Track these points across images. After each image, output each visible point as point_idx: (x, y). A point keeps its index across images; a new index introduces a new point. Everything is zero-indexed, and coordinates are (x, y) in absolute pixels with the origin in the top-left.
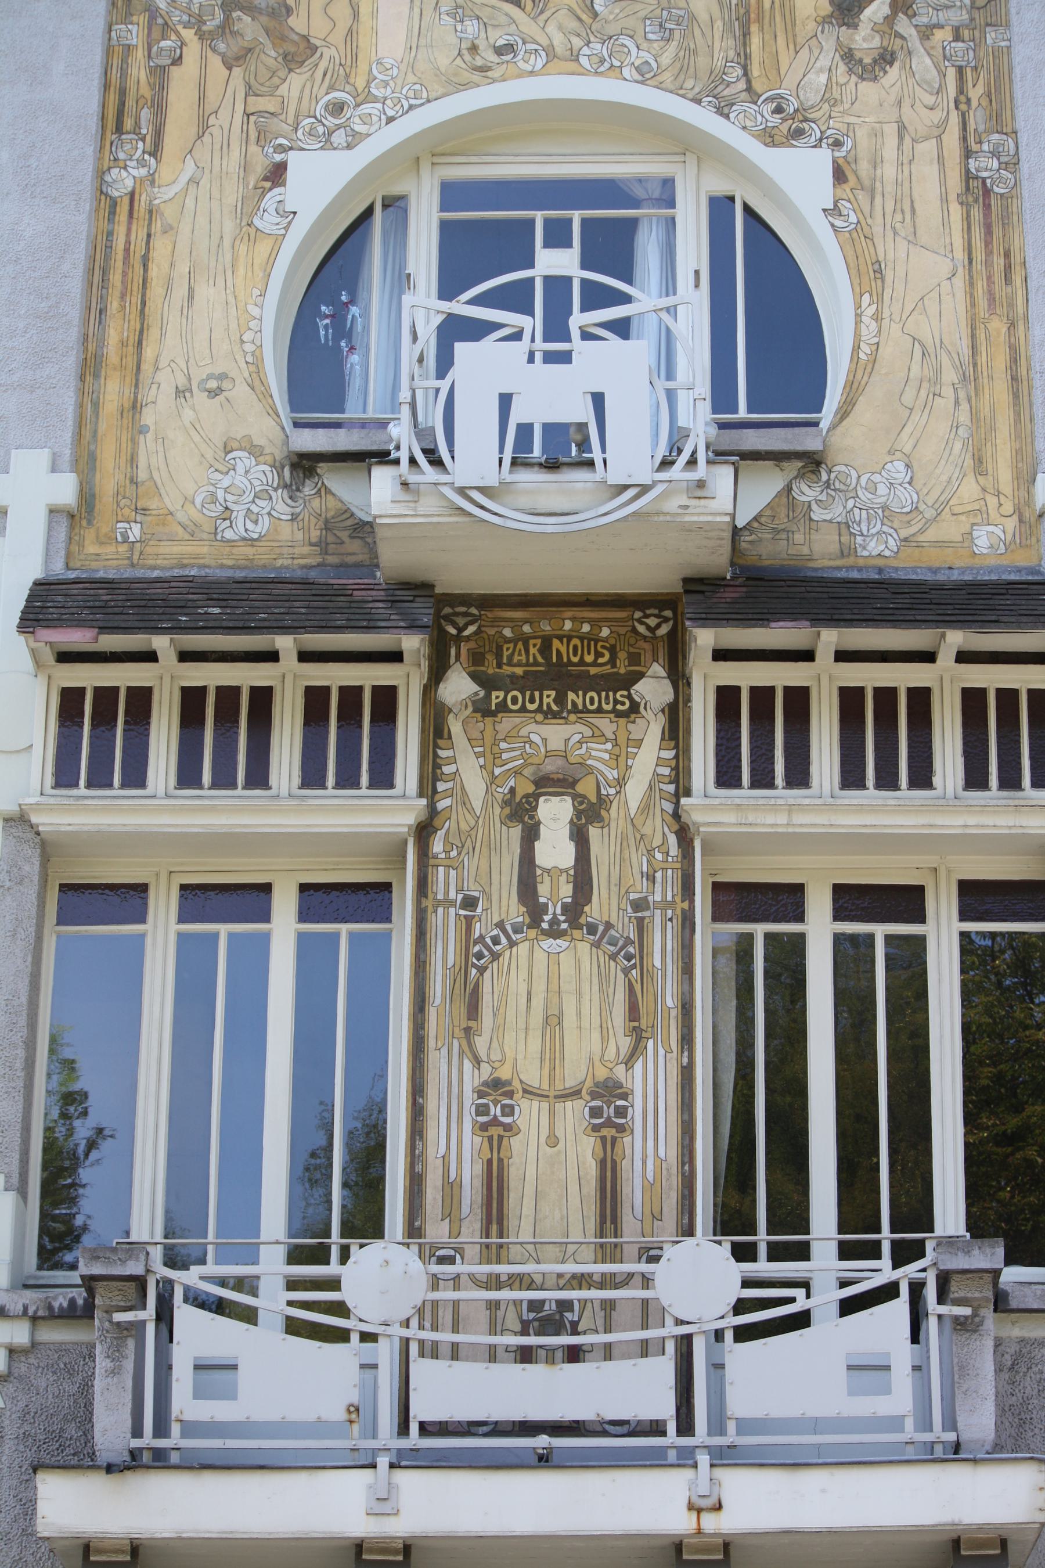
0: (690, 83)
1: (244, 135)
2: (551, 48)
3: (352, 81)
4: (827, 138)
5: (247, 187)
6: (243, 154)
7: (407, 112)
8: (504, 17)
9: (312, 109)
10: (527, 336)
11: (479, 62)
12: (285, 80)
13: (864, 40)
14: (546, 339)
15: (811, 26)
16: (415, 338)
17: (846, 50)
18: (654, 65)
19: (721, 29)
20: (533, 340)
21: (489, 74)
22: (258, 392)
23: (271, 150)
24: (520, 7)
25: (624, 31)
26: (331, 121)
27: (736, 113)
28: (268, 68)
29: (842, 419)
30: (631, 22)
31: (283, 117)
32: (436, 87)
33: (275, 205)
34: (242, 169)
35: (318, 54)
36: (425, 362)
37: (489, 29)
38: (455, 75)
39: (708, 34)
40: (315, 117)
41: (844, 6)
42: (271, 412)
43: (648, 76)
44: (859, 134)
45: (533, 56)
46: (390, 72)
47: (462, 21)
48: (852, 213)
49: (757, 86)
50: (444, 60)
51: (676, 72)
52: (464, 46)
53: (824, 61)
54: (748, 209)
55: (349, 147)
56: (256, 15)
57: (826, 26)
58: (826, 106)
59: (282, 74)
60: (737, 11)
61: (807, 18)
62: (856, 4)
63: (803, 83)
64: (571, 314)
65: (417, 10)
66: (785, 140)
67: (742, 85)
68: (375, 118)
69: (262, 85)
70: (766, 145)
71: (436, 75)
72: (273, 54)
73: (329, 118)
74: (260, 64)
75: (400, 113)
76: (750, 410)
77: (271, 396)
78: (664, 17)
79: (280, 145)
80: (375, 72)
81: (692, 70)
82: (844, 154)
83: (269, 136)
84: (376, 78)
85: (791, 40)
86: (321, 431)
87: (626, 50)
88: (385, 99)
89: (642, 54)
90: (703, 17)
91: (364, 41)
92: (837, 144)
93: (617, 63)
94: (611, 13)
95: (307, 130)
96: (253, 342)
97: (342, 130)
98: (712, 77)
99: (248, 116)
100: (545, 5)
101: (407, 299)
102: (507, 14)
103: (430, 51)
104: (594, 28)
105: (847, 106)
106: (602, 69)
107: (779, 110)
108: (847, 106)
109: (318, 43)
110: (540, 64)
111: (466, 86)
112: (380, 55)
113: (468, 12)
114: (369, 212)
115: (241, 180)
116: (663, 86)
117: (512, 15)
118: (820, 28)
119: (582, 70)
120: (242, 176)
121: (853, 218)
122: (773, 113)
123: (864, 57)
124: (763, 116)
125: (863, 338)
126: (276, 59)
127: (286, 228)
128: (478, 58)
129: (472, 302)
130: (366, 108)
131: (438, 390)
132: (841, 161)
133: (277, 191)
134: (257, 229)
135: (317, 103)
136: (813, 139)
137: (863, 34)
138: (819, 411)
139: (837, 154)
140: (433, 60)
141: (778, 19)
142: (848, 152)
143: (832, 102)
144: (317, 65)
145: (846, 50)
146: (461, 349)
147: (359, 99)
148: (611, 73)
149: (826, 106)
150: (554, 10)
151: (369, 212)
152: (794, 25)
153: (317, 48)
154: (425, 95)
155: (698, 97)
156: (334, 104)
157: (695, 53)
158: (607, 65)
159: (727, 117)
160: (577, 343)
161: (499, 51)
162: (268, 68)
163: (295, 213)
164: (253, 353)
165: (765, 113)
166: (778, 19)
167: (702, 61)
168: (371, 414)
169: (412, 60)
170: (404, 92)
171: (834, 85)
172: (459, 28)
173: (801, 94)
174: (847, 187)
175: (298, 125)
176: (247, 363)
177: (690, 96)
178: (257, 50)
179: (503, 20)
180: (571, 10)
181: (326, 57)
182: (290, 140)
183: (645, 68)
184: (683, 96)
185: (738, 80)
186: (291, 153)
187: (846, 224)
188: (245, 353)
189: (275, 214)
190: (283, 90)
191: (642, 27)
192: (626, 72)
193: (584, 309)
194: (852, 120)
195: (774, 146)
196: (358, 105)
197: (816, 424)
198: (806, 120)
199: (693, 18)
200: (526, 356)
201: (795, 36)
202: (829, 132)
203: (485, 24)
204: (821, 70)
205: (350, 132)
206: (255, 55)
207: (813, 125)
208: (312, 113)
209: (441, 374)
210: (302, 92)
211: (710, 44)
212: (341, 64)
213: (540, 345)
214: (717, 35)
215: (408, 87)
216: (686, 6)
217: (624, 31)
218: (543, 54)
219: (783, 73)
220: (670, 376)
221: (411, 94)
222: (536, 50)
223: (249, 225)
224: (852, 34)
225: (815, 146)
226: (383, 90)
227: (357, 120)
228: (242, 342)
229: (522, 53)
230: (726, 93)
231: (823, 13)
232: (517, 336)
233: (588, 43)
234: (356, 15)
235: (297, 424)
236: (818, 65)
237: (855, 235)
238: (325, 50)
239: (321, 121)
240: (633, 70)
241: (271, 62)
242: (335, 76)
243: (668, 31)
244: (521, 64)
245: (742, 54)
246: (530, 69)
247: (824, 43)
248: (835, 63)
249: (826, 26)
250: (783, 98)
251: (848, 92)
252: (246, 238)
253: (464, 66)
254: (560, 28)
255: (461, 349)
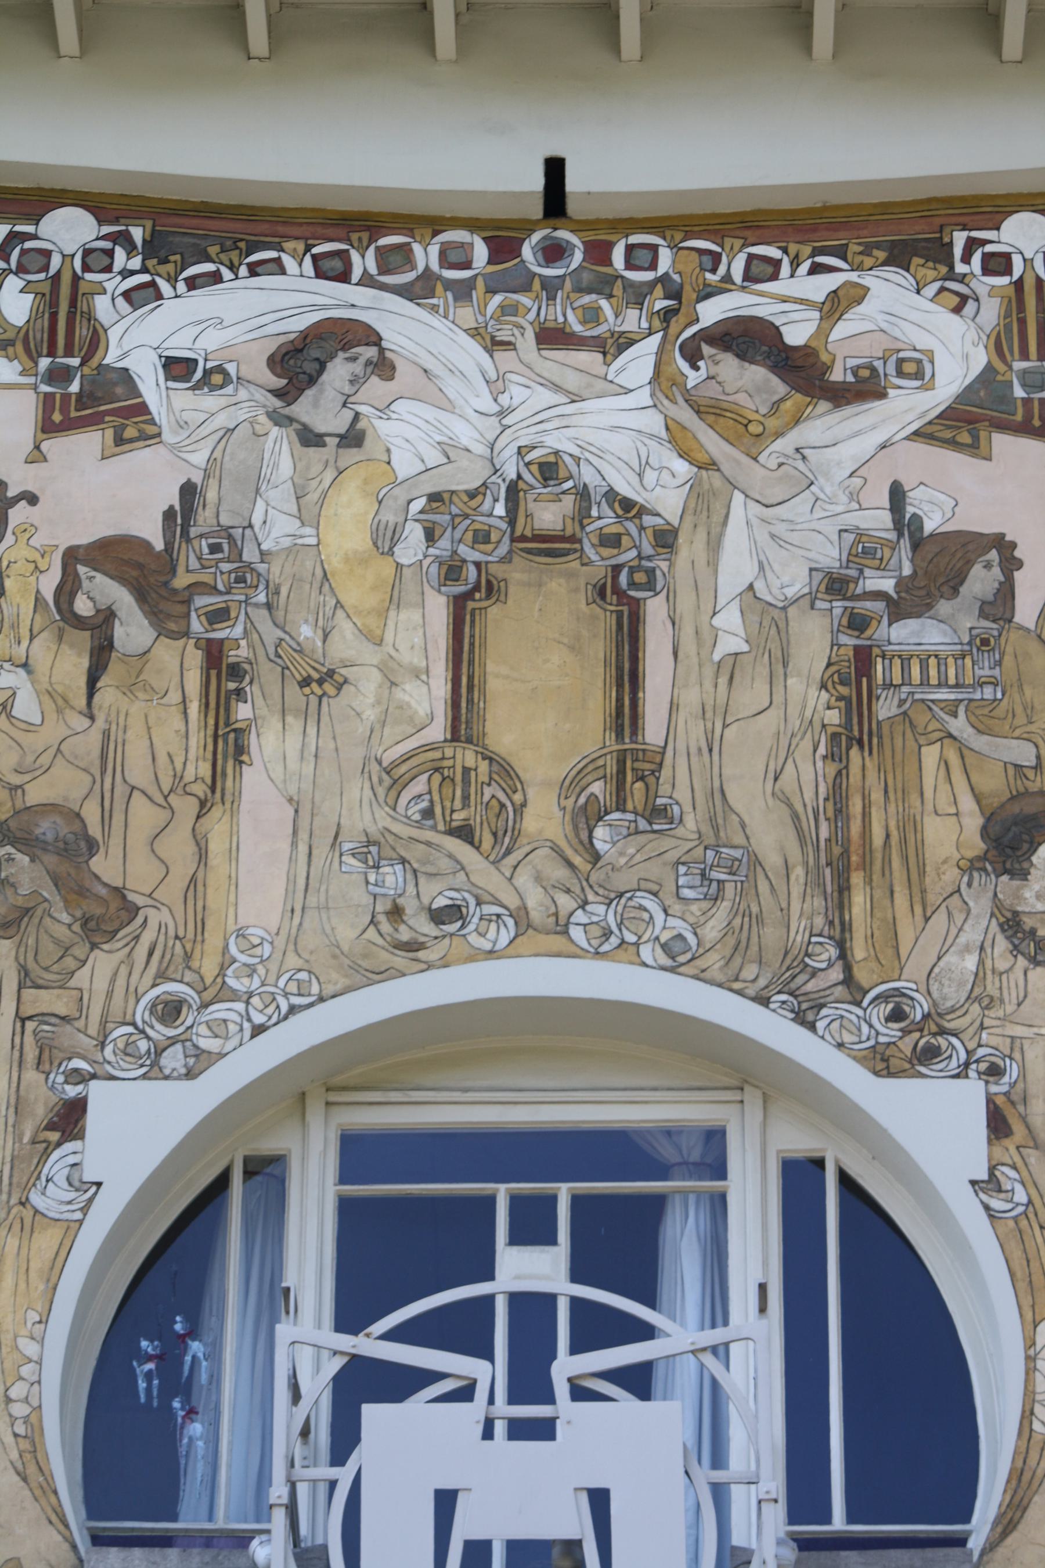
0: (750, 971)
1: (16, 1054)
2: (522, 913)
3: (195, 964)
4: (977, 1061)
5: (21, 1140)
6: (14, 1085)
7: (286, 1018)
8: (447, 860)
9: (129, 1012)
10: (481, 1393)
11: (405, 935)
12: (84, 962)
13: (1038, 897)
14: (514, 1399)
15: (951, 874)
16: (296, 1396)
17: (1009, 915)
18: (692, 940)
19: (802, 880)
20: (491, 1401)
21: (421, 954)
22: (34, 1485)
23: (61, 1079)
24: (472, 843)
25: (644, 885)
26: (160, 1032)
27: (827, 1021)
28: (57, 942)
29: (1005, 1534)
30: (654, 870)
31: (80, 1024)
32: (334, 976)
33: (66, 1171)
34: (12, 1110)
35: (139, 920)
36: (312, 1436)
37: (422, 880)
38: (365, 956)
39: (781, 888)
40: (134, 1024)
41: (1006, 840)
42: (54, 1518)
43: (682, 959)
44: (1029, 1055)
45: (493, 926)
46: (258, 951)
47: (377, 867)
48: (1018, 1187)
49: (861, 975)
50: (346, 932)
51: (728, 953)
52: (379, 908)
53: (972, 934)
54: (846, 1181)
55: (190, 1074)
56: (39, 852)
57: (976, 874)
58: (976, 1009)
59: (80, 951)
60: (829, 850)
61: (945, 862)
62: (1025, 837)
63: (936, 970)
64: (554, 1357)
65: (303, 848)
66: (907, 1066)
67: (836, 974)
68: (233, 1028)
69: (46, 969)
70: (877, 1073)
71: (334, 957)
72: (65, 918)
73: (158, 1026)
74: (44, 937)
75: (274, 1019)
76: (851, 1519)
77: (55, 1492)
78: (709, 862)
79: (76, 1070)
80: (233, 950)
81: (754, 948)
82: (1005, 1088)
83: (58, 1055)
84: (234, 961)
85: (917, 899)
86: (137, 1552)
87: (646, 916)
88: (251, 995)
89: (672, 922)
90: (772, 859)
91: (214, 899)
92: (994, 1072)
93: (631, 938)
94: (622, 854)
95: (121, 1044)
96: (26, 1400)
97: (179, 1047)
98: (788, 962)
99: (23, 1021)
100: (514, 840)
101: (284, 1331)
102: (451, 856)
103: (324, 916)
104: (593, 878)
105: (1010, 1008)
106: (606, 947)
107: (897, 1015)
108: (1010, 1008)
109: (140, 901)
110: (504, 939)
111: (383, 974)
112: (242, 922)
113: (387, 852)
114: (222, 1182)
115: (10, 1129)
116: (706, 975)
117: (460, 857)
118: (966, 879)
119: (574, 949)
120: (11, 1121)
121: (1021, 1196)
122: (889, 1019)
123: (1038, 925)
124: (871, 1026)
125: (1038, 1397)
126: (69, 926)
127: (85, 1210)
128: (402, 928)
129: (389, 1336)
130: (219, 1011)
131: (333, 1484)
132: (1000, 1101)
133: (69, 1147)
134: (36, 1211)
135: (138, 1001)
136: (954, 1063)
137: (1037, 887)
138: (967, 1519)
139: (994, 1089)
140: (328, 931)
141: (896, 863)
142: (1013, 1085)
143: (986, 1001)
144: (137, 938)
145: (1009, 915)
146: (372, 1414)
147: (208, 996)
148: (620, 951)
149: (976, 1009)
150: (528, 849)
151: (222, 1182)
152: (922, 873)
153: (138, 909)
154: (315, 989)
155: (765, 993)
156: (166, 1003)
157: (760, 920)
158: (614, 941)
159: (812, 1027)
160: (564, 1406)
161: (438, 917)
162: (57, 942)
163: (99, 1184)
164: (26, 1420)
165: (875, 1021)
166: (896, 863)
167: (771, 935)
168: (221, 1522)
169: (294, 931)
170: (281, 983)
171: (989, 973)
172: (372, 878)
173: (934, 988)
174: (1010, 1144)
175: (106, 1037)
176: (16, 1435)
177: (751, 992)
178: (39, 912)
179: (444, 864)
180: (555, 849)
181: (153, 924)
182: (92, 1062)
183: (677, 946)
184: (739, 993)
185: (830, 965)
186: (93, 1083)
187: (1009, 1206)
188: (13, 1419)
189: (66, 1185)
190: (81, 978)
191: (673, 877)
192: (646, 953)
193: (577, 1348)
194: (1019, 1031)
195: (890, 1073)
196: (205, 1005)
197: (960, 1542)
198: (942, 1032)
199: (756, 862)
200: (480, 1429)
201: (923, 891)
202: (981, 1052)
203: (415, 871)
204: (967, 949)
205: (192, 1051)
206: (36, 920)
207: (954, 1041)
208: (129, 1018)
209: (340, 1455)
210: (113, 980)
211: (784, 905)
212: (177, 937)
213: (503, 1408)
214: (796, 890)
215: (287, 976)
216: (744, 842)
217: (644, 885)
218: (510, 922)
219: (904, 952)
220: (718, 1461)
221: (293, 987)
222: (498, 916)
223: (22, 1204)
224: (1019, 888)
225: (957, 1076)
226: (246, 981)
227: (203, 1030)
228: (8, 1400)
229: (475, 920)
230: (810, 987)
231: (970, 854)
232: (465, 1393)
233: (584, 904)
234: (202, 854)
235: (98, 1540)
236: (962, 939)
237: (1024, 1223)
238: (151, 912)
239: (143, 1032)
240: (659, 950)
241: (61, 932)
242: (168, 957)
243: (714, 885)
244: (474, 939)
245: (837, 921)
246: (488, 946)
247: (971, 904)
248: (990, 936)
249: (976, 874)
250: (904, 995)
251: (1012, 985)
252: (17, 1226)
253: (380, 941)
254: (538, 879)
255: (372, 1414)
